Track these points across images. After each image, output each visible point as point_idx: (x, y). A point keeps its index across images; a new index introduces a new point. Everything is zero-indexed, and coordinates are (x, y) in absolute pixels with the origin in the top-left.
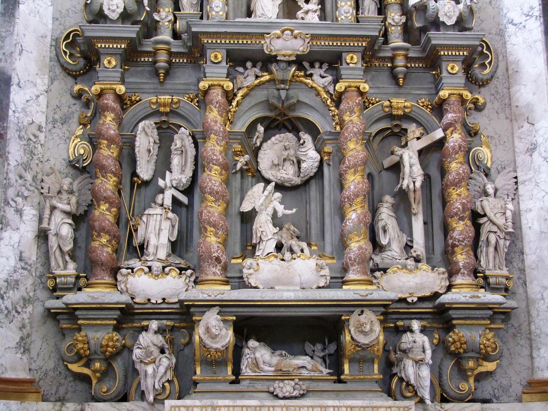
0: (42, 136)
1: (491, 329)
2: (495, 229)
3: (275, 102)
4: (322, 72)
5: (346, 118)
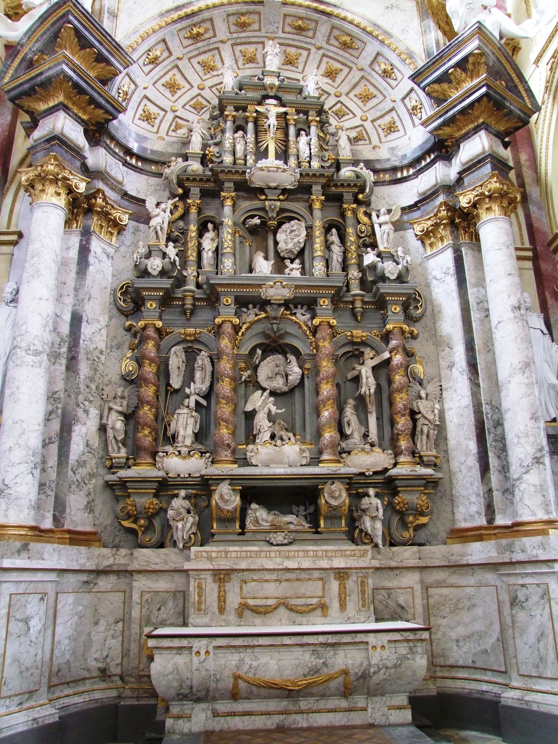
0: (103, 358)
1: (425, 494)
2: (427, 422)
3: (269, 332)
4: (303, 311)
5: (321, 344)
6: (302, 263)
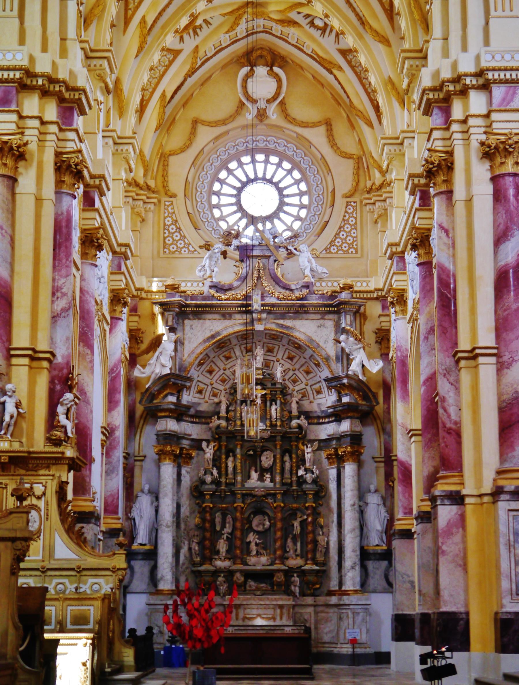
6: (272, 474)
